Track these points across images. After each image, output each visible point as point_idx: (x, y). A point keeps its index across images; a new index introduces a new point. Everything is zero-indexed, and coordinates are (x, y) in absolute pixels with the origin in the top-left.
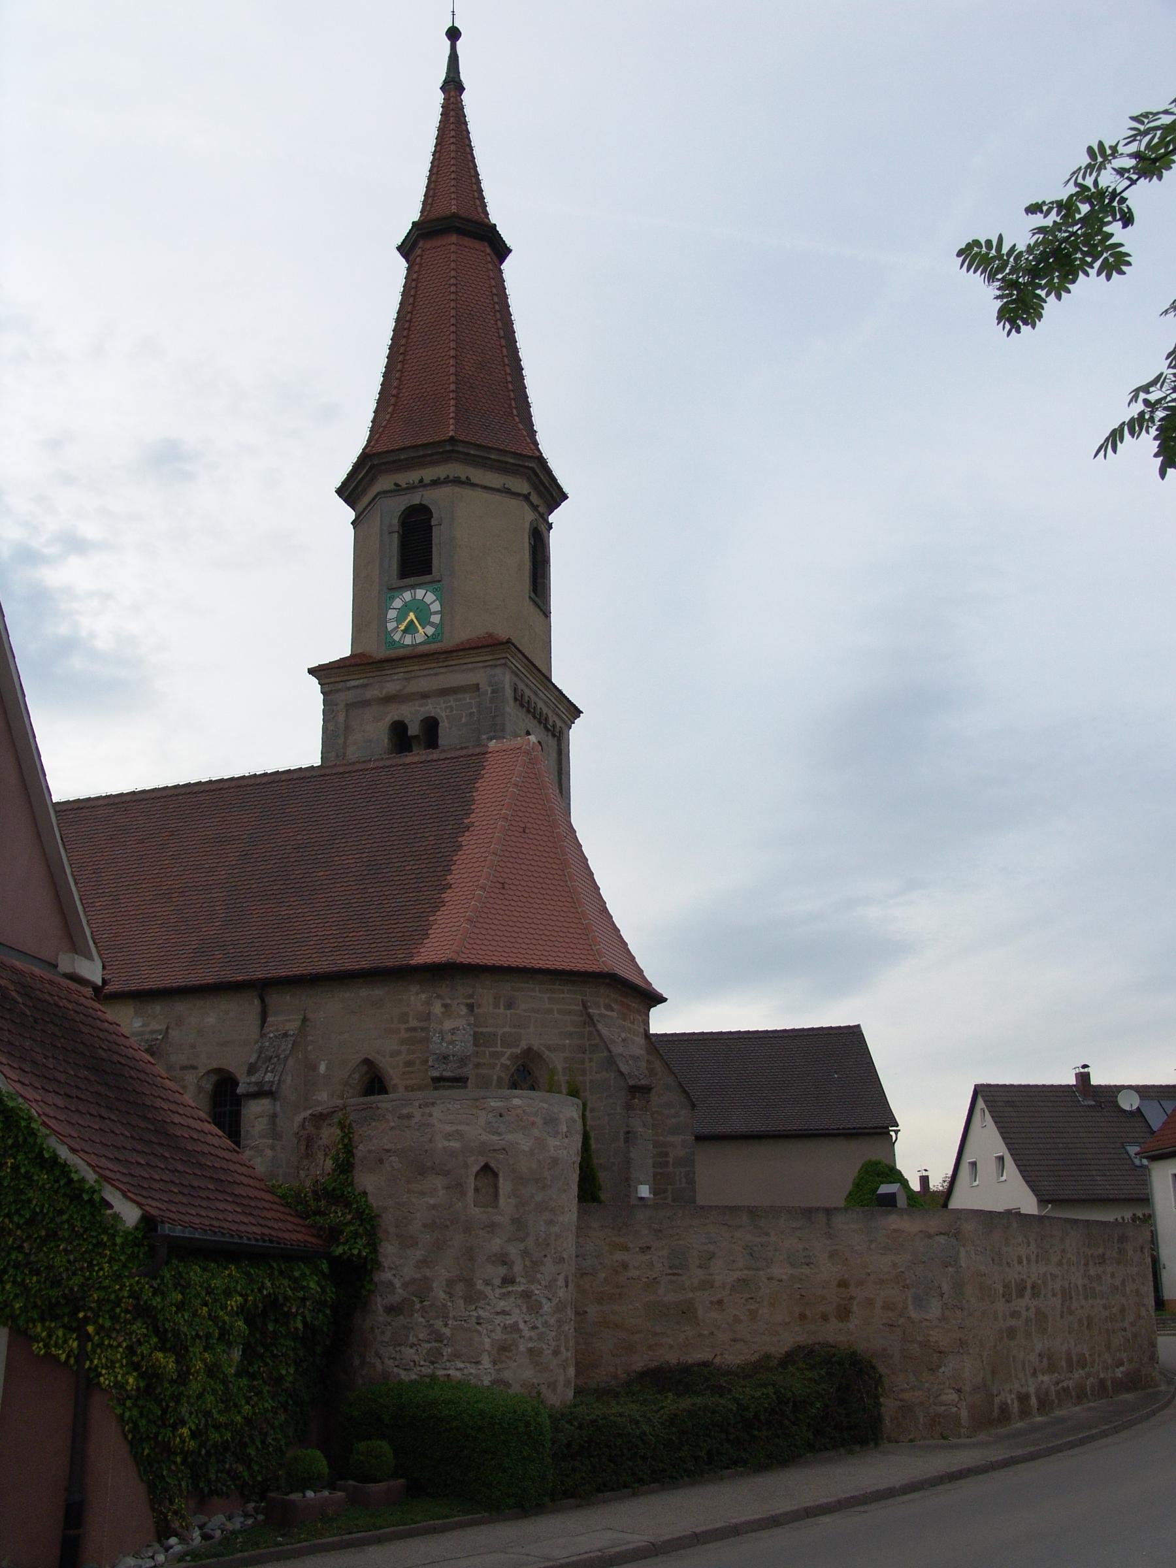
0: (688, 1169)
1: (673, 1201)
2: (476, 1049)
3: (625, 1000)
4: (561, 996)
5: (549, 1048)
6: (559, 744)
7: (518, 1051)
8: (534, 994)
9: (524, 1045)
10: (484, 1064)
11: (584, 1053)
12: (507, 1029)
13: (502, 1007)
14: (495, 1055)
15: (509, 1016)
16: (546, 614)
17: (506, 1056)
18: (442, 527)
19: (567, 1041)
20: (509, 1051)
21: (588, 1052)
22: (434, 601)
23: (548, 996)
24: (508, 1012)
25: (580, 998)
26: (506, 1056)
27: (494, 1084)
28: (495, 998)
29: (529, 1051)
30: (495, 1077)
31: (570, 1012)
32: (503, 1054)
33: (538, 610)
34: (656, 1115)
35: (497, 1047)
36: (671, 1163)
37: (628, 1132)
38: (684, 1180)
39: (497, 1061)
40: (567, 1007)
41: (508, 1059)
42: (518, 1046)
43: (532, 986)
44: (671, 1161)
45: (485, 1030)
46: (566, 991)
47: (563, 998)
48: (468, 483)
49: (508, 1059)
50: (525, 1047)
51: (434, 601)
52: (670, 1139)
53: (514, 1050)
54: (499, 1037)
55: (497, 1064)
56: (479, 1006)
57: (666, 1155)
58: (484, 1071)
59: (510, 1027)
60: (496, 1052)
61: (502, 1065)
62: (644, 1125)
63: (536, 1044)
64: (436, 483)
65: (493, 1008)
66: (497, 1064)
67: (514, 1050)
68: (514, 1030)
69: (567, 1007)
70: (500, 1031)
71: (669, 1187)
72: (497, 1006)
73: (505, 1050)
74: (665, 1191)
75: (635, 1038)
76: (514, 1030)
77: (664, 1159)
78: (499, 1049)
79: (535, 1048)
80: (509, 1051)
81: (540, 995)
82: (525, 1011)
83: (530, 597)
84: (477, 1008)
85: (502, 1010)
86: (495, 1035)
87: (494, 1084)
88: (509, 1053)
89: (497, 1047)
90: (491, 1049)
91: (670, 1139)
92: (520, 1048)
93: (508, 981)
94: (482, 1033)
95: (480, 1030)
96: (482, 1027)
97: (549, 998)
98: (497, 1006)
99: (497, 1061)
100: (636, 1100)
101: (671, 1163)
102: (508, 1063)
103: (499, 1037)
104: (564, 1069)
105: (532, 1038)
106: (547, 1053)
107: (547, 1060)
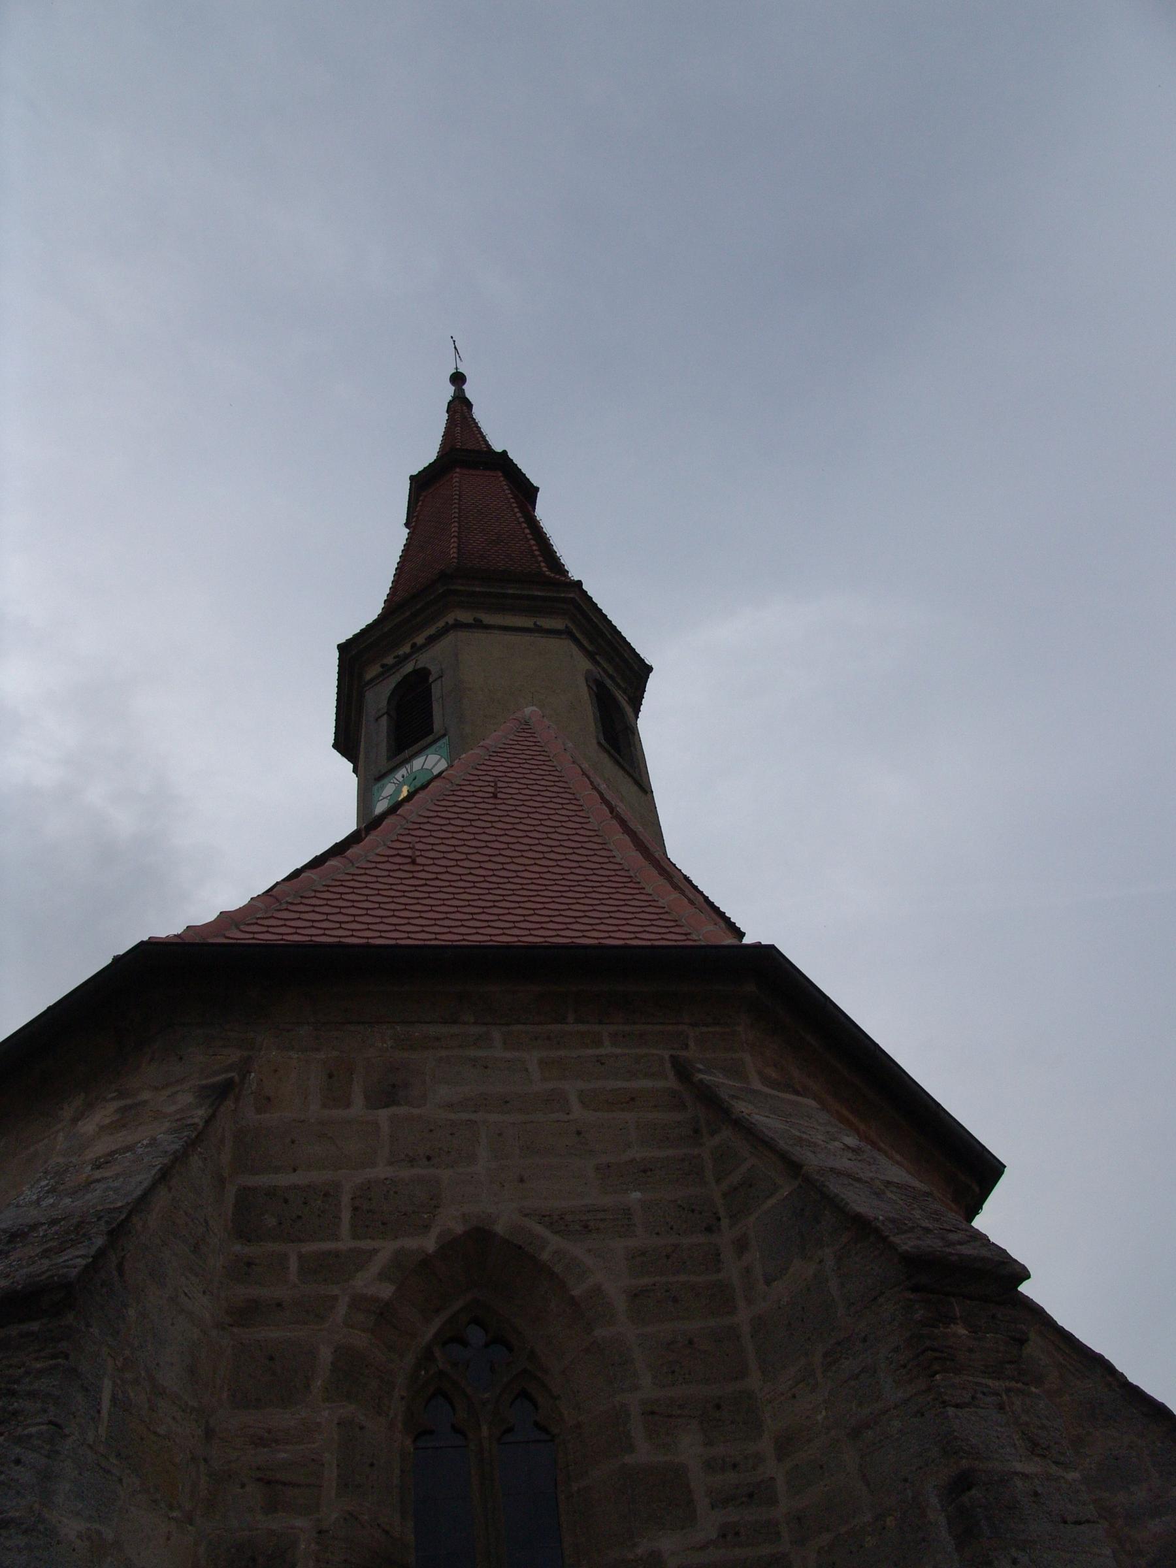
7: (429, 1244)
11: (709, 1229)
12: (382, 1171)
13: (358, 1101)
16: (645, 789)
17: (375, 1268)
18: (443, 679)
19: (637, 1195)
20: (387, 1249)
21: (725, 1222)
22: (439, 760)
24: (383, 1114)
26: (375, 1268)
28: (331, 1076)
30: (326, 1354)
33: (630, 780)
37: (963, 1482)
39: (335, 1290)
40: (620, 1084)
42: (427, 1227)
45: (283, 1180)
48: (479, 625)
50: (459, 1229)
51: (439, 760)
53: (411, 1243)
54: (346, 1199)
55: (335, 1298)
60: (337, 1254)
62: (1035, 1448)
64: (432, 640)
65: (324, 1106)
66: (335, 1298)
67: (411, 1243)
78: (345, 1243)
79: (499, 1228)
80: (387, 1249)
81: (508, 1055)
83: (599, 744)
90: (308, 1248)
92: (435, 1231)
95: (264, 1180)
99: (335, 1290)
102: (386, 1291)
103: (346, 1199)
106: (555, 1241)
107: (558, 1269)
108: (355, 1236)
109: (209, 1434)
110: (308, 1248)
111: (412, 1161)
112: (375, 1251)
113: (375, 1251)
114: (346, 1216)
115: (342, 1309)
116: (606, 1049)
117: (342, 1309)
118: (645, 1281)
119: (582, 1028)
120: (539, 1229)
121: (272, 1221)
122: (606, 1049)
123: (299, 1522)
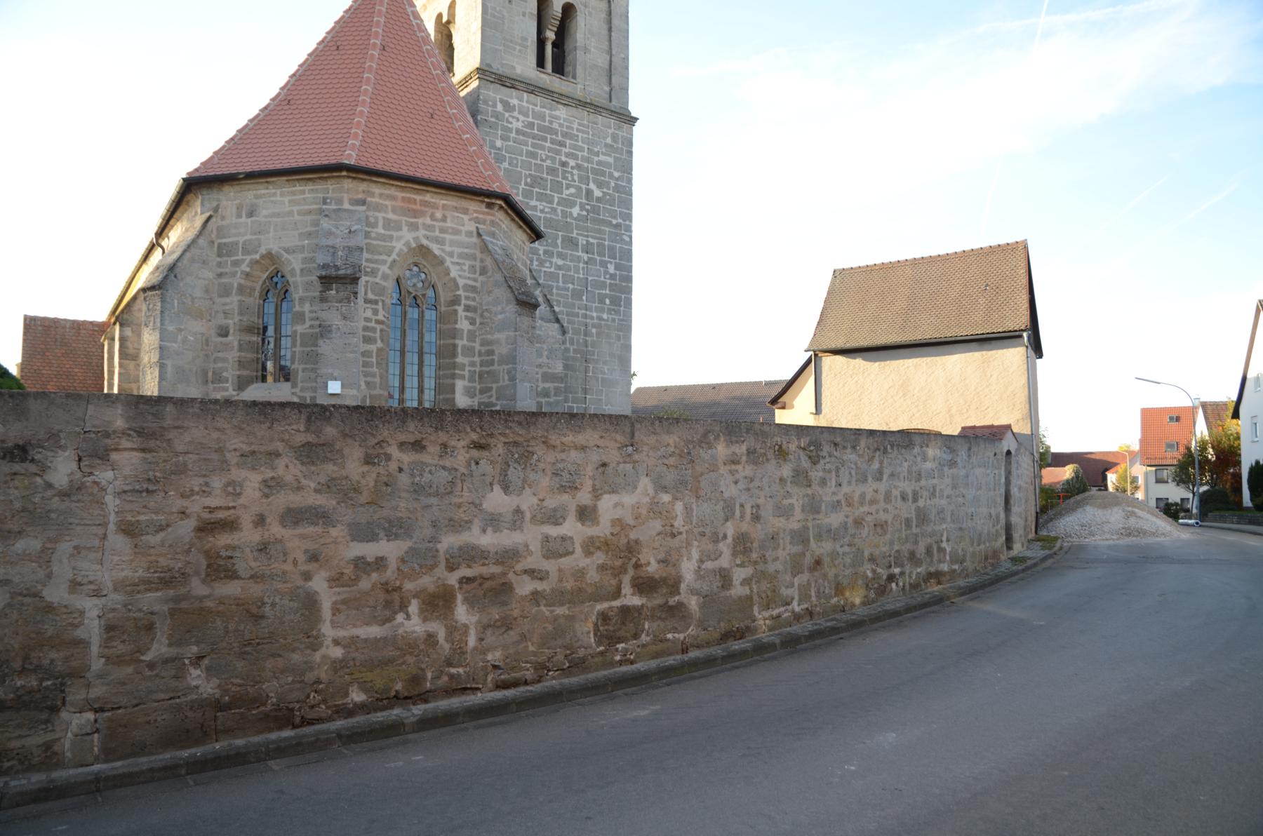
0: (511, 366)
1: (497, 399)
2: (219, 259)
3: (418, 198)
4: (302, 196)
5: (287, 251)
6: (610, 6)
8: (272, 199)
9: (263, 250)
10: (226, 273)
12: (248, 237)
13: (244, 216)
14: (236, 263)
15: (249, 224)
19: (306, 242)
20: (248, 258)
23: (290, 198)
24: (250, 220)
25: (321, 195)
27: (234, 292)
29: (270, 256)
30: (236, 285)
31: (310, 212)
32: (243, 261)
34: (485, 314)
35: (238, 255)
36: (496, 360)
38: (506, 377)
39: (237, 269)
41: (248, 266)
43: (274, 191)
44: (496, 358)
46: (307, 191)
47: (304, 199)
49: (248, 266)
50: (264, 252)
52: (497, 336)
54: (240, 245)
56: (223, 218)
57: (491, 353)
58: (224, 280)
59: (251, 234)
60: (238, 260)
61: (242, 272)
63: (275, 248)
68: (254, 237)
69: (306, 207)
70: (242, 239)
71: (494, 386)
72: (239, 216)
73: (244, 257)
74: (491, 389)
75: (448, 237)
76: (254, 237)
77: (491, 357)
78: (240, 257)
80: (248, 258)
81: (281, 199)
82: (266, 217)
84: (222, 220)
85: (244, 219)
86: (237, 244)
87: (234, 292)
88: (247, 261)
89: (238, 255)
90: (233, 258)
91: (497, 336)
93: (249, 190)
94: (225, 244)
95: (224, 241)
96: (225, 238)
97: (290, 201)
98: (239, 216)
100: (333, 292)
101: (496, 360)
102: (248, 269)
103: (240, 245)
104: (302, 270)
105: (271, 243)
106: (286, 255)
108: (242, 255)
109: (214, 303)
110: (233, 258)
111: (255, 234)
112: (245, 260)
113: (245, 260)
114: (241, 249)
115: (239, 274)
116: (307, 195)
117: (239, 274)
118: (305, 266)
119: (301, 188)
120: (283, 252)
121: (225, 251)
122: (307, 195)
123: (231, 322)
